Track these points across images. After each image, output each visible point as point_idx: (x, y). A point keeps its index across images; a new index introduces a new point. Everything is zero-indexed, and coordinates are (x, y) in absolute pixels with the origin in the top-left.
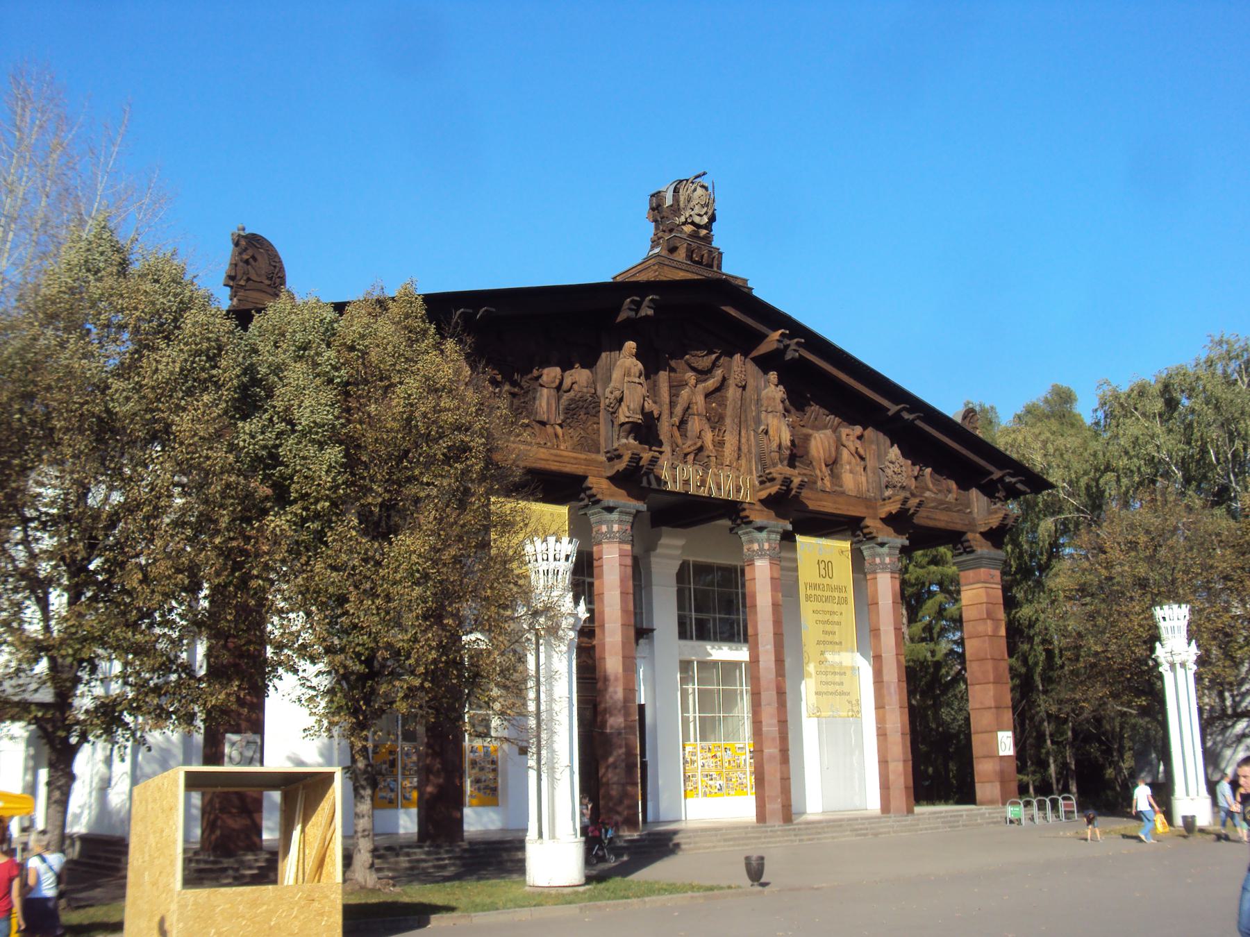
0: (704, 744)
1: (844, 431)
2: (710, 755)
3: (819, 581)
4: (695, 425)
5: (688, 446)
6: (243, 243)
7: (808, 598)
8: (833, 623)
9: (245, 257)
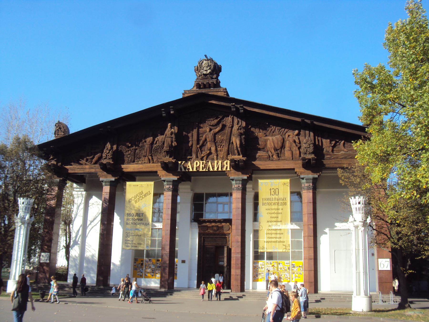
0: (268, 261)
2: (271, 265)
3: (269, 197)
6: (57, 125)
7: (263, 204)
8: (278, 213)
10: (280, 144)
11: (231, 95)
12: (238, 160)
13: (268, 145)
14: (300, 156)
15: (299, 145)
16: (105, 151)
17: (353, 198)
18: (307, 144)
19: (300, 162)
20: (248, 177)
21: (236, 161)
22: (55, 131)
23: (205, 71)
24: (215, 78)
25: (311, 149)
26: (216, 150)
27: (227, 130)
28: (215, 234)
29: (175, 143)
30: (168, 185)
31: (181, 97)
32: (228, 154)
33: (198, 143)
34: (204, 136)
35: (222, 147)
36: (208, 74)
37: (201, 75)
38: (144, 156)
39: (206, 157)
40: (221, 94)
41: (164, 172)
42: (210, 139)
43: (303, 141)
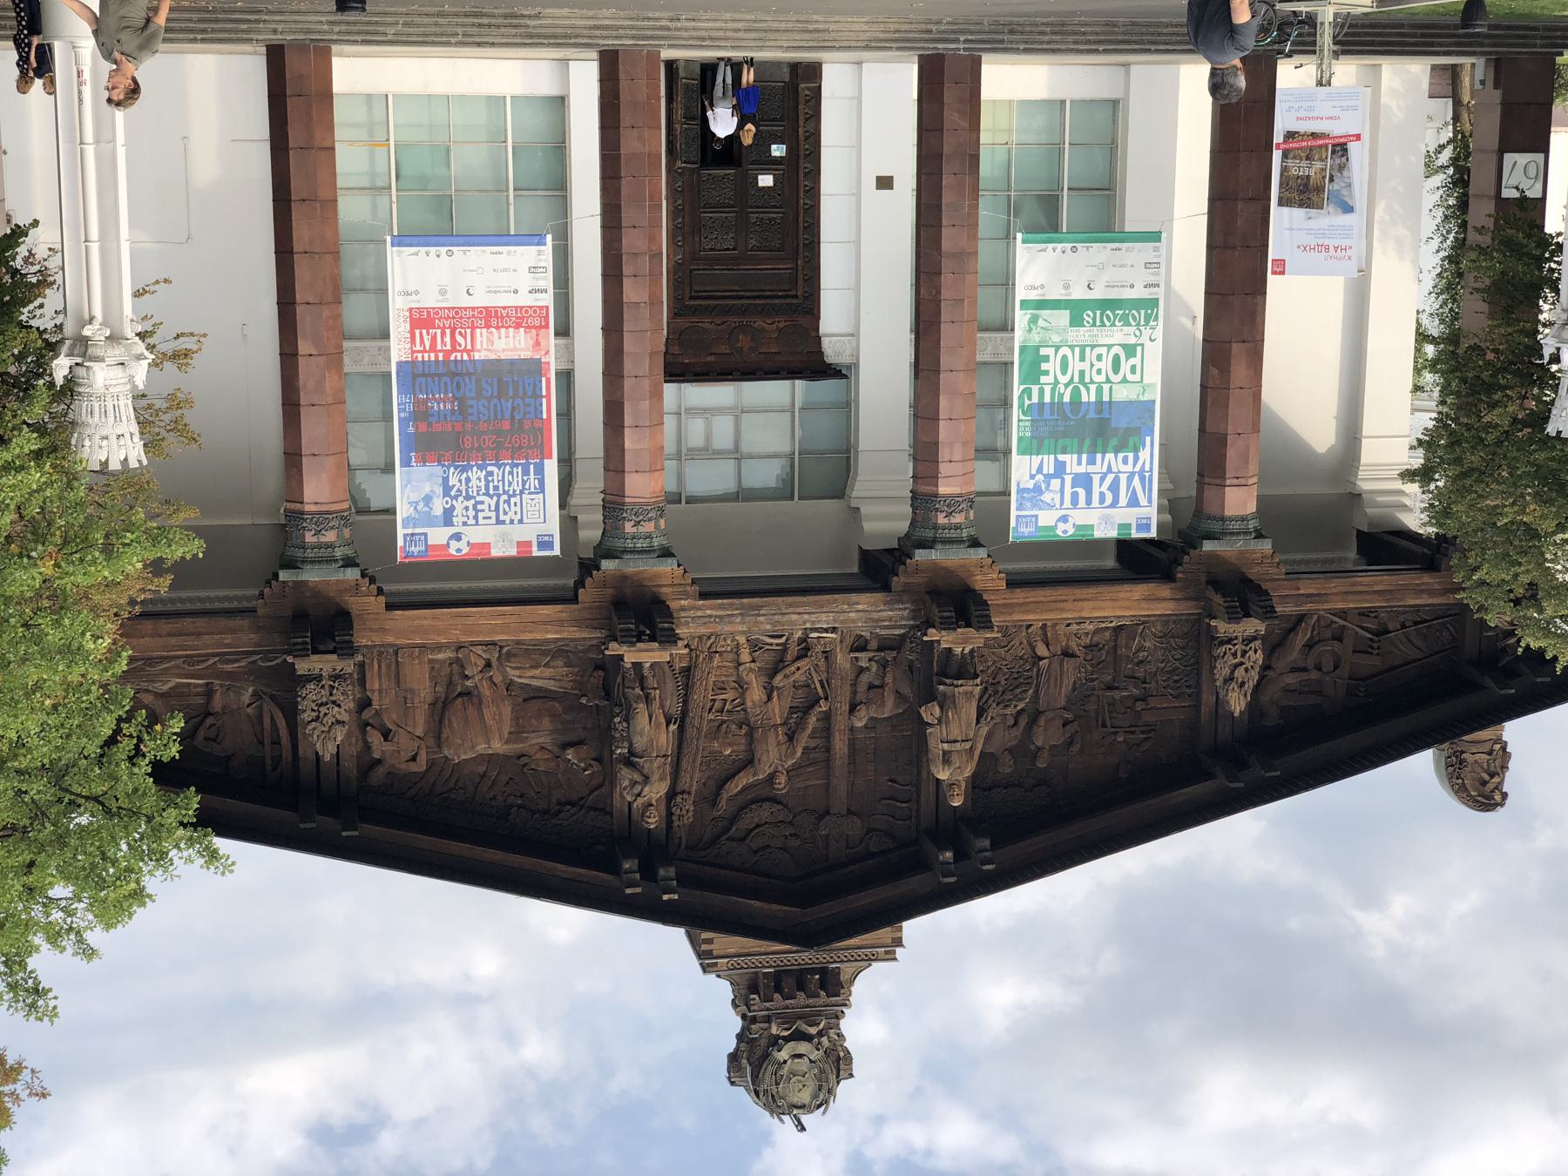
1: (421, 766)
4: (778, 710)
5: (799, 672)
9: (1496, 780)
10: (455, 718)
11: (677, 935)
12: (639, 640)
13: (507, 711)
14: (362, 666)
15: (367, 714)
16: (1255, 675)
17: (133, 464)
18: (329, 720)
19: (361, 640)
20: (598, 569)
21: (652, 639)
22: (1504, 767)
23: (800, 1056)
24: (754, 1020)
25: (310, 695)
26: (742, 687)
27: (692, 779)
28: (744, 311)
29: (927, 718)
30: (958, 527)
31: (913, 928)
32: (687, 672)
33: (827, 717)
34: (799, 754)
35: (718, 705)
36: (787, 1039)
37: (820, 1034)
38: (1072, 655)
39: (789, 657)
40: (724, 943)
41: (980, 582)
42: (772, 740)
43: (348, 735)
